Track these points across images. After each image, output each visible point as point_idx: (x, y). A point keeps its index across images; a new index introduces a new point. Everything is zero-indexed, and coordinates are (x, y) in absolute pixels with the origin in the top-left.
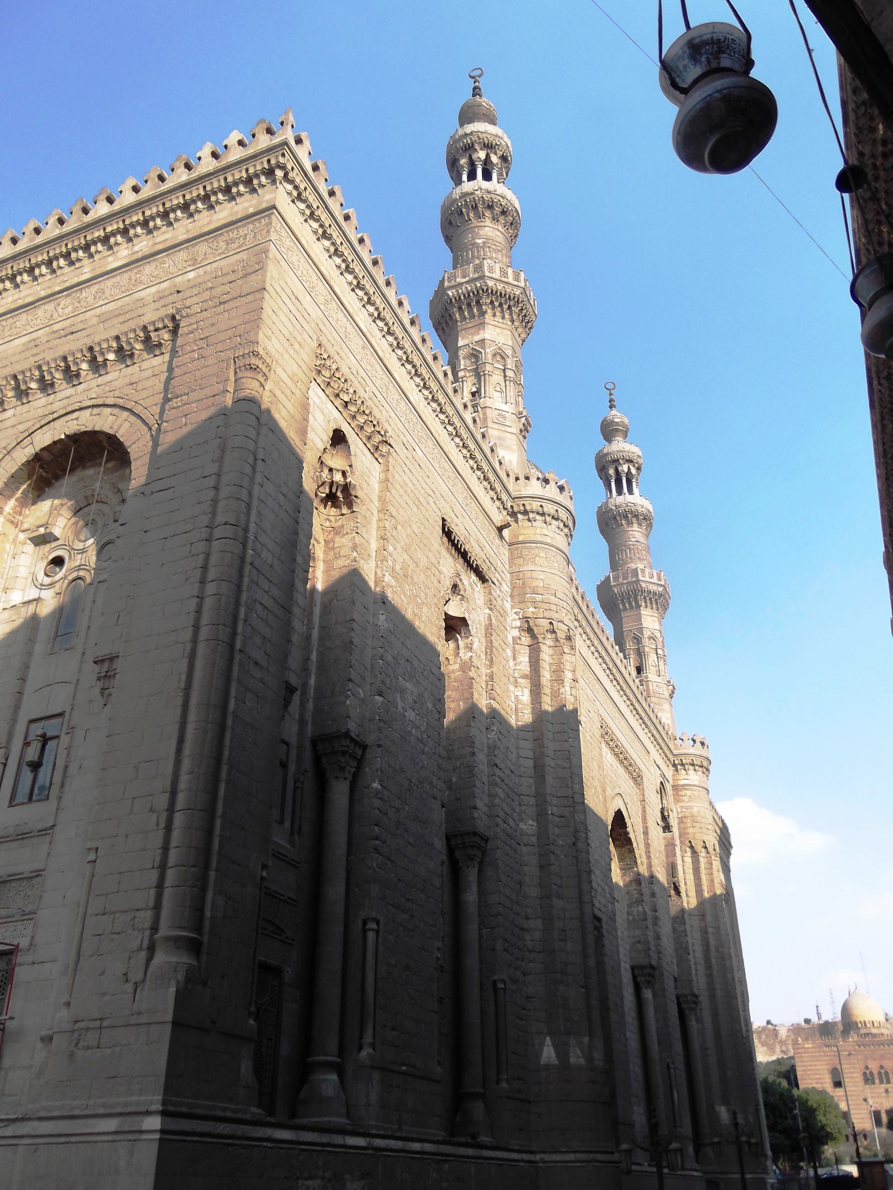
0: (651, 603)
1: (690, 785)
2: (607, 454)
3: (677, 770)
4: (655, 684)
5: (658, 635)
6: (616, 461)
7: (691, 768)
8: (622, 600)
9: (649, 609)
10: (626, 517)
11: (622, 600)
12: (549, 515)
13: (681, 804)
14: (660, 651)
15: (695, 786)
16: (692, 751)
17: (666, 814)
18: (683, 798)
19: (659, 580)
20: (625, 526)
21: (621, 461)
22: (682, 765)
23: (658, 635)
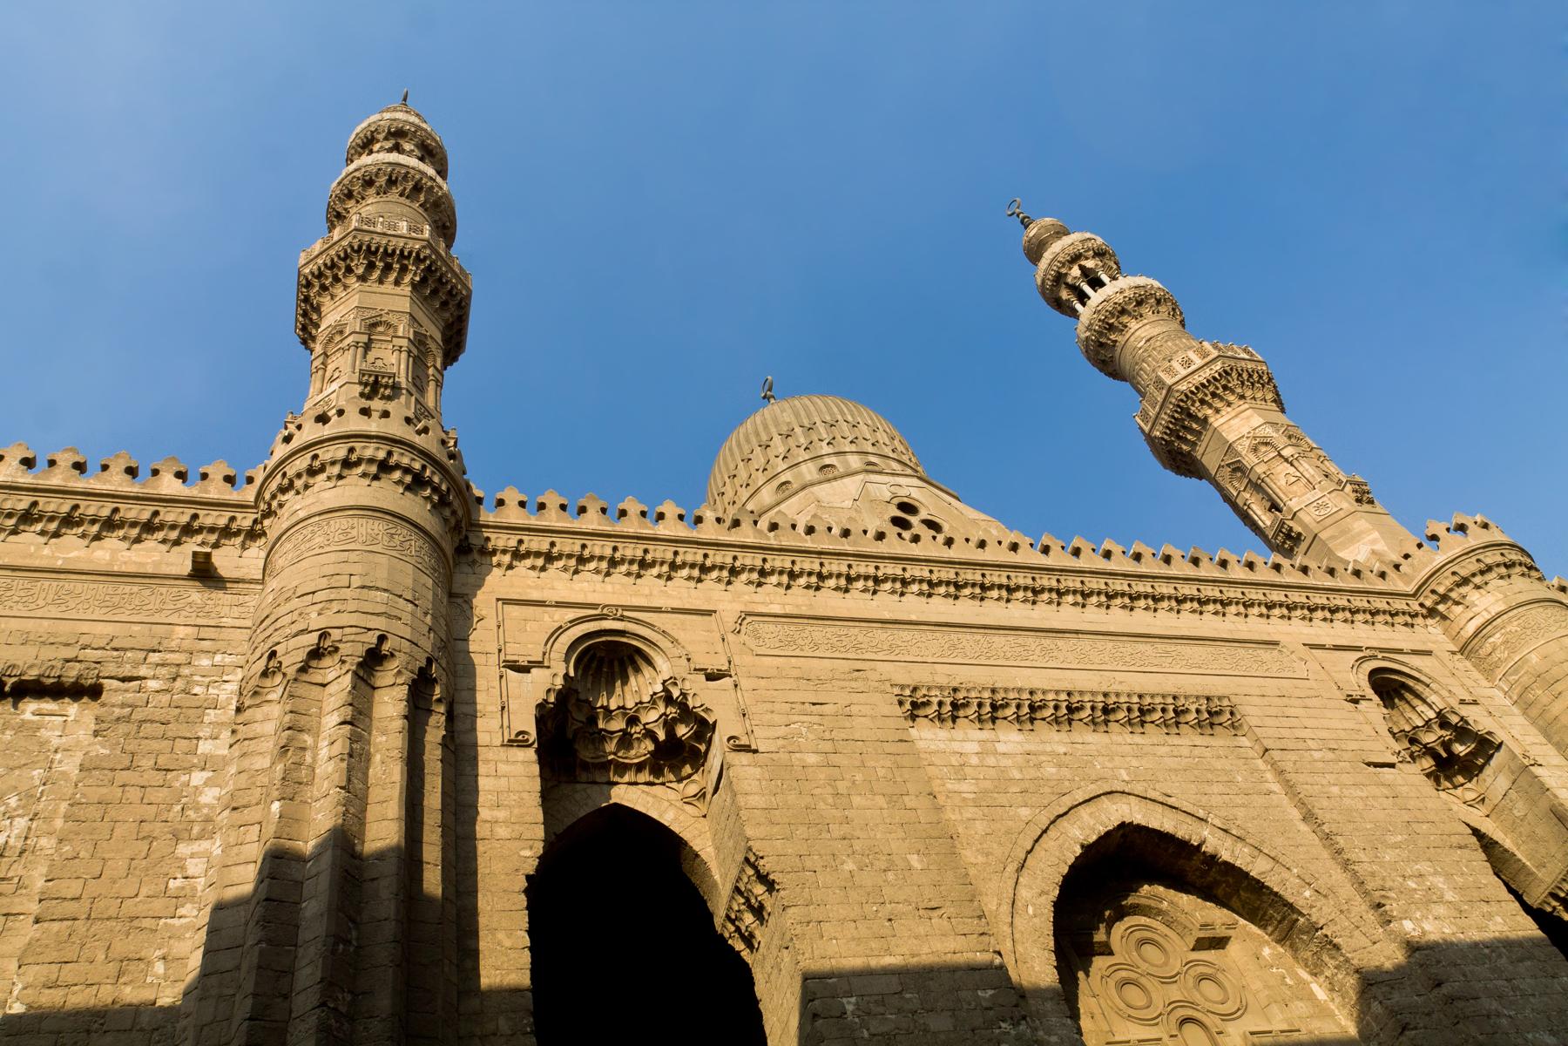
0: (1222, 399)
1: (1489, 622)
2: (1043, 281)
3: (1444, 618)
4: (1311, 509)
5: (1268, 431)
6: (1059, 278)
7: (1464, 590)
8: (1179, 438)
9: (1225, 410)
10: (1111, 328)
11: (1179, 438)
12: (299, 476)
13: (1499, 673)
14: (1286, 452)
15: (1499, 615)
16: (1440, 559)
17: (1454, 719)
18: (1495, 657)
19: (1204, 355)
20: (1119, 338)
21: (1063, 271)
22: (1444, 598)
23: (1268, 431)
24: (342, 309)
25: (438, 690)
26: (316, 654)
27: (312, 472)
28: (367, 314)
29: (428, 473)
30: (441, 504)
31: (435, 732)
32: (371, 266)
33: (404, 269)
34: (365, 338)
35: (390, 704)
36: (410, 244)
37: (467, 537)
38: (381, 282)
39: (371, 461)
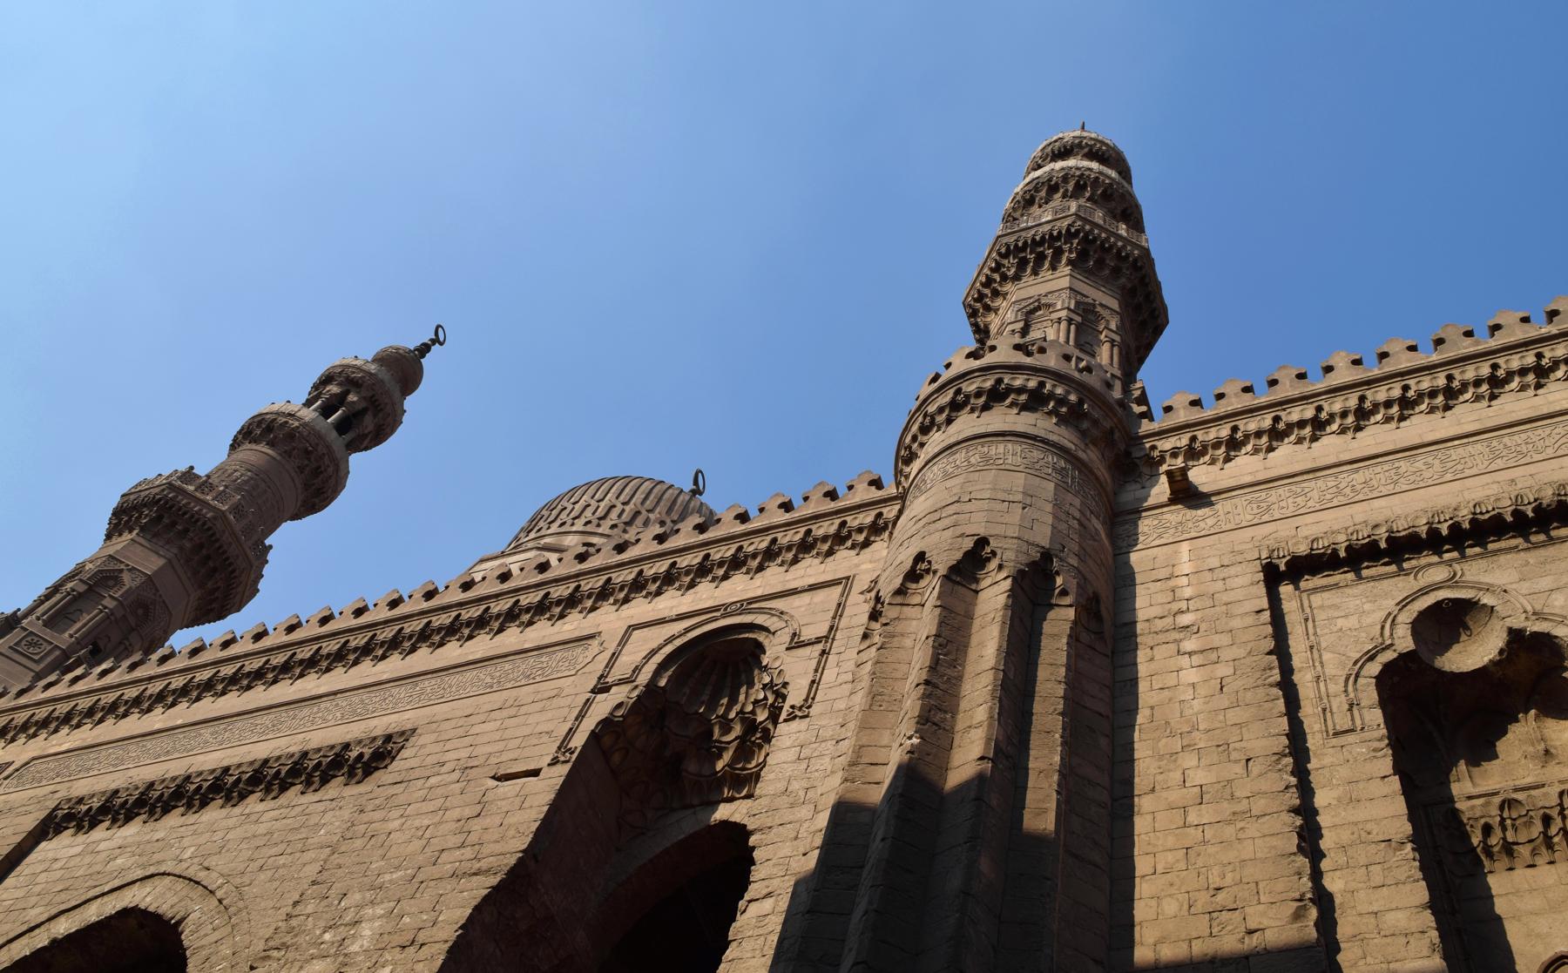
24: (1004, 317)
25: (1059, 581)
26: (913, 576)
27: (925, 430)
28: (1024, 304)
29: (1048, 386)
30: (1072, 417)
31: (1060, 621)
32: (1022, 264)
33: (1058, 253)
34: (1021, 324)
35: (994, 594)
36: (1058, 224)
37: (1128, 454)
38: (1035, 273)
39: (978, 394)
